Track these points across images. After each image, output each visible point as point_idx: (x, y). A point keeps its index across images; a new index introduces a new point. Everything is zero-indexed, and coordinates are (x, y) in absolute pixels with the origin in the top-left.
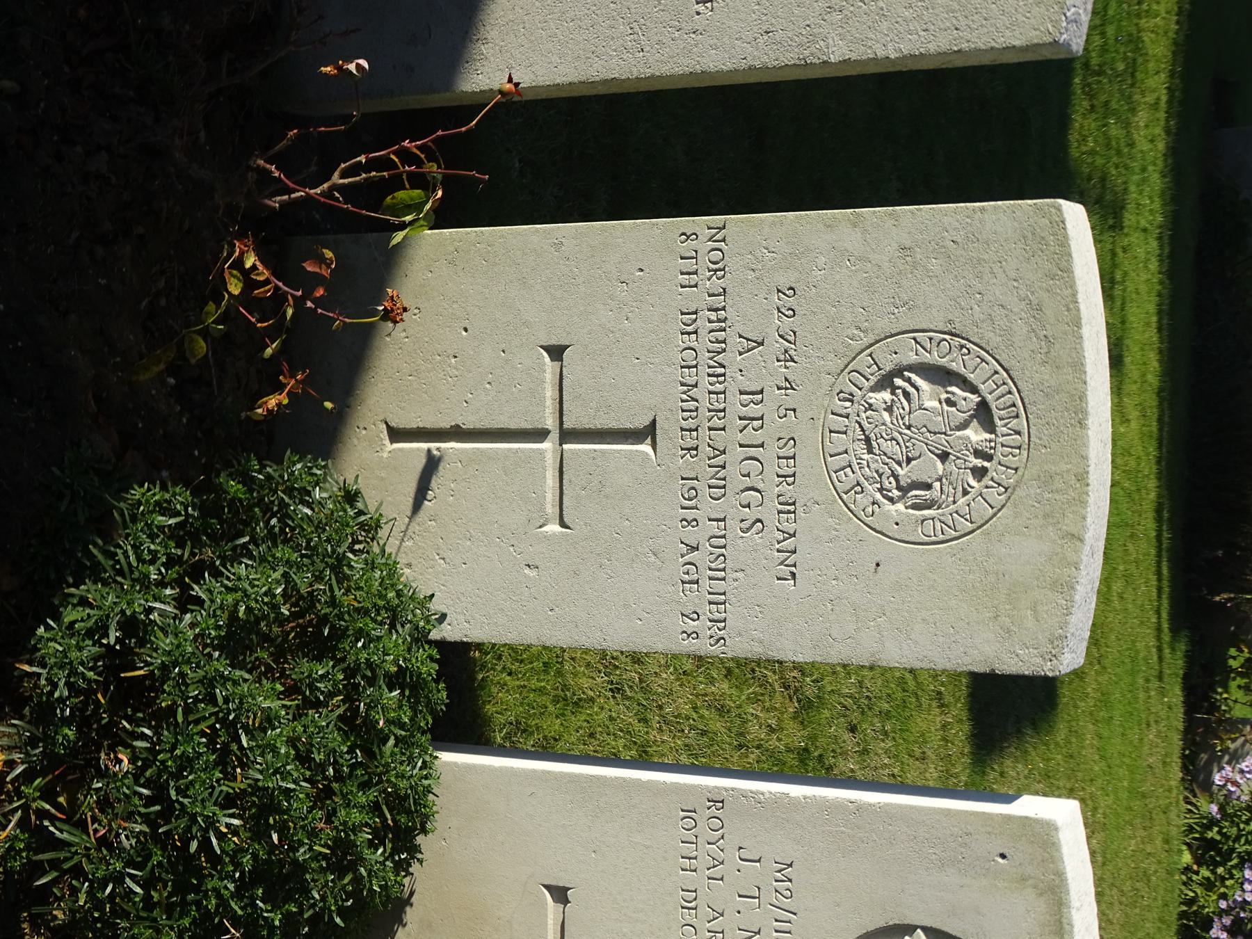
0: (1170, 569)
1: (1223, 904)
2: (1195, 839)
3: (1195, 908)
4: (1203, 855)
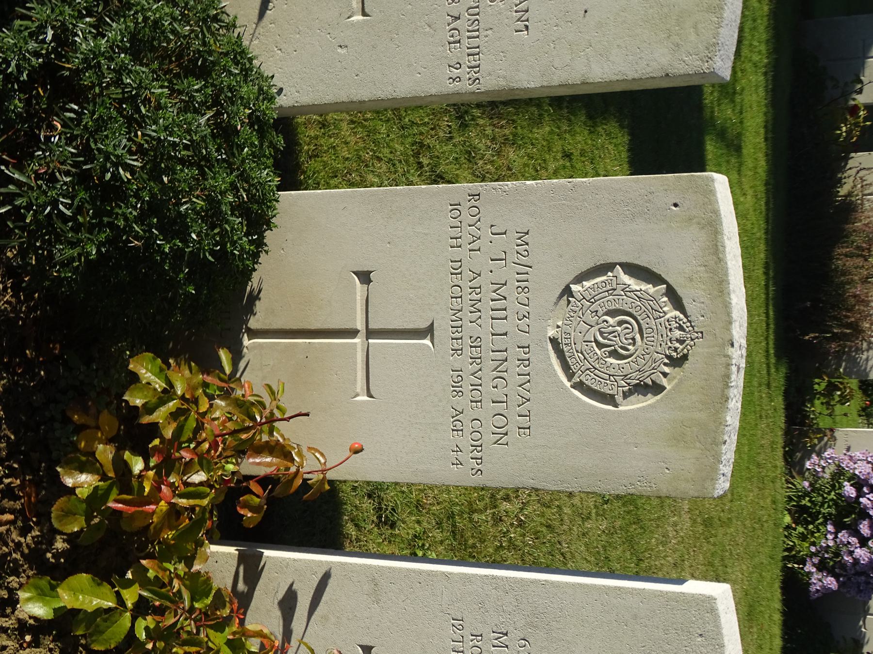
0: (774, 311)
1: (813, 549)
2: (793, 506)
3: (794, 553)
4: (799, 518)
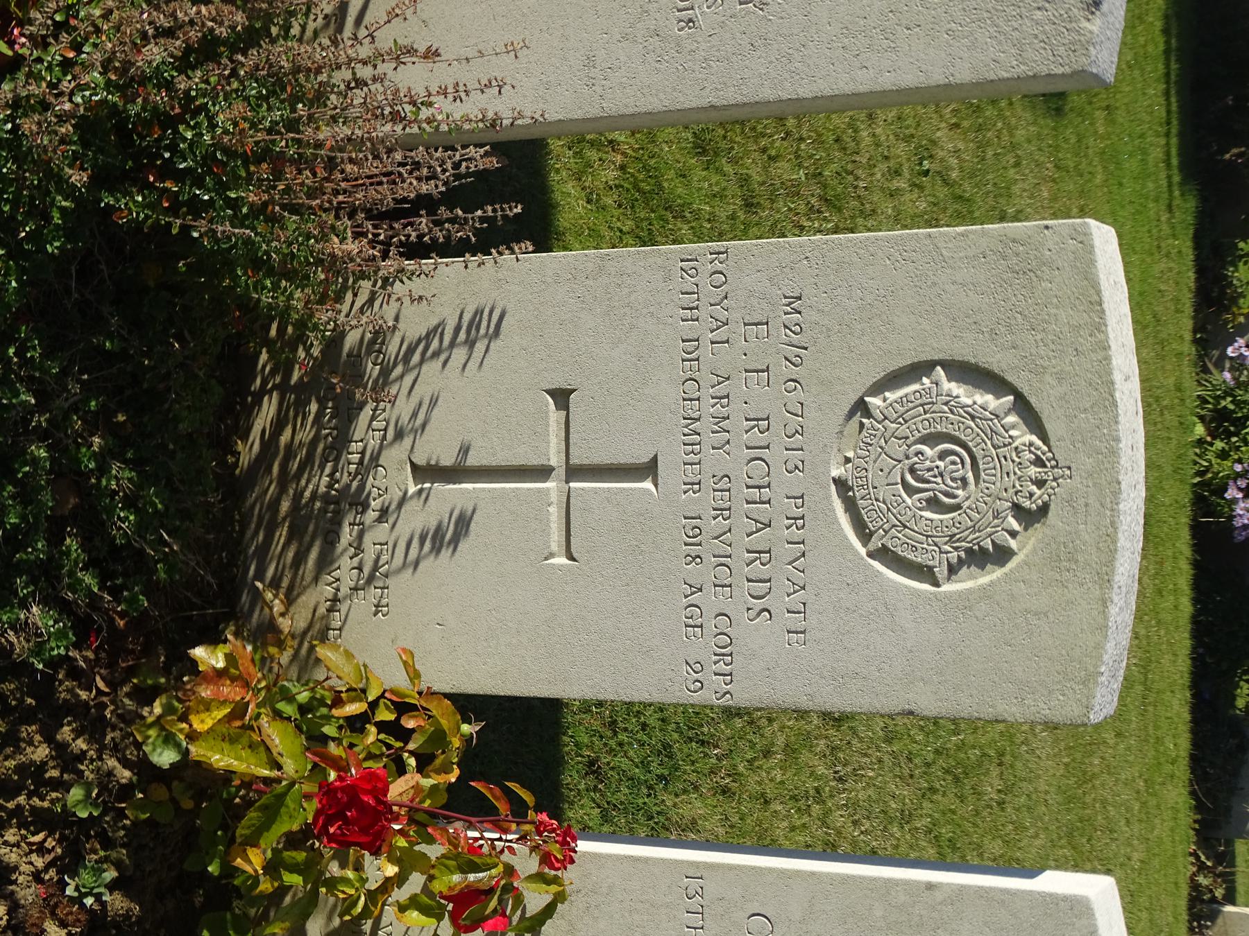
1: (1238, 468)
4: (1217, 428)
